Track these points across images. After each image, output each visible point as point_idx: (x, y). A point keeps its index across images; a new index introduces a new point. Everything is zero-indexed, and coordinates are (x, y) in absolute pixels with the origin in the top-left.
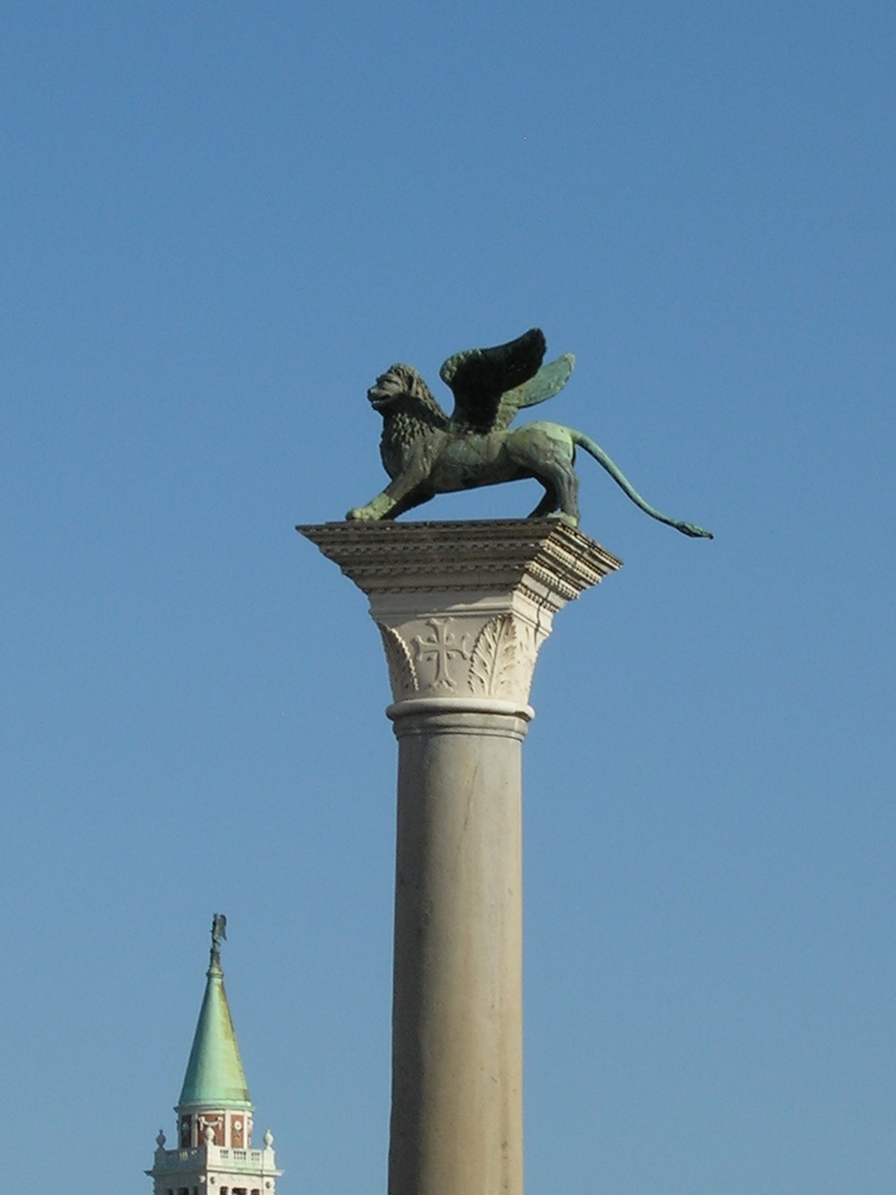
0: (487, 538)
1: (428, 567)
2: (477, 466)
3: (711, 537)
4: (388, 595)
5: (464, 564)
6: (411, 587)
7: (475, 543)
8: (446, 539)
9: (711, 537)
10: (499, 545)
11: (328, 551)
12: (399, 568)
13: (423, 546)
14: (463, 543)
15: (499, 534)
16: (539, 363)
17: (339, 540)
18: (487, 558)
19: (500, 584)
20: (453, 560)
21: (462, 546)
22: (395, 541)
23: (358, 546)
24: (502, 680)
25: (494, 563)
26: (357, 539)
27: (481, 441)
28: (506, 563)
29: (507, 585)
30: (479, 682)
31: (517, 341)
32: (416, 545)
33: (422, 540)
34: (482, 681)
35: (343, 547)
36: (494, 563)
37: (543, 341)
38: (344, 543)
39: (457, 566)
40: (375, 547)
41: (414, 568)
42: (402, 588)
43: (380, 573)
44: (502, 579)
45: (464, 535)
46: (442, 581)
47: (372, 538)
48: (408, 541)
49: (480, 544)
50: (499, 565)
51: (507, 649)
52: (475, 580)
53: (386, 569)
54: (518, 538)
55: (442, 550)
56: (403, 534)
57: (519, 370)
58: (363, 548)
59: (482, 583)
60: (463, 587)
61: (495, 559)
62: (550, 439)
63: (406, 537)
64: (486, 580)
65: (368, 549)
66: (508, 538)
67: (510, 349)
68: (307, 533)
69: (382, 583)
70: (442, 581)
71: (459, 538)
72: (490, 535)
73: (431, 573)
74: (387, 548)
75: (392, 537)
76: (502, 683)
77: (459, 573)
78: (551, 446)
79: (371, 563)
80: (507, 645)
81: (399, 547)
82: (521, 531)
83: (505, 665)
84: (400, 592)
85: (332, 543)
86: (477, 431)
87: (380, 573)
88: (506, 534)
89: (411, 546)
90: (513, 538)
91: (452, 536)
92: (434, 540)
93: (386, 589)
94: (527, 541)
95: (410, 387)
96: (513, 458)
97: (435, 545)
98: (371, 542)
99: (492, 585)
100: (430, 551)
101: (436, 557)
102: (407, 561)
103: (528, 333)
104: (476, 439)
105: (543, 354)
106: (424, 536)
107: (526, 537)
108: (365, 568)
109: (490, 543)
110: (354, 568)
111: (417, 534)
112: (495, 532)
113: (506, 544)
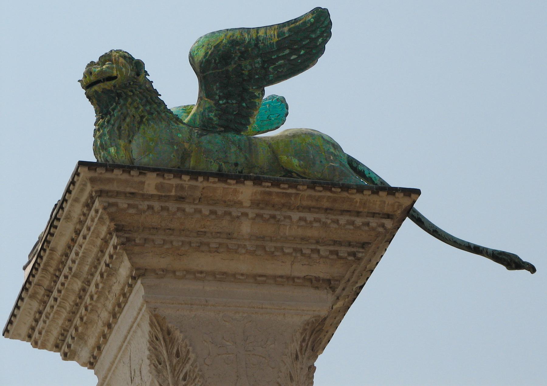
0: (319, 209)
2: (236, 165)
3: (532, 269)
6: (201, 272)
7: (302, 215)
9: (532, 269)
11: (110, 205)
13: (235, 212)
16: (321, 50)
17: (128, 190)
19: (318, 279)
21: (285, 217)
25: (319, 247)
27: (238, 137)
28: (332, 248)
29: (324, 280)
31: (296, 20)
32: (226, 209)
35: (131, 202)
36: (319, 247)
40: (173, 206)
42: (188, 272)
44: (321, 270)
46: (243, 265)
49: (310, 217)
50: (324, 250)
54: (358, 214)
57: (293, 57)
58: (157, 205)
59: (296, 274)
61: (317, 242)
62: (328, 142)
66: (343, 212)
67: (286, 29)
68: (92, 174)
70: (243, 265)
72: (326, 204)
74: (189, 209)
75: (198, 194)
78: (332, 150)
84: (183, 277)
88: (346, 207)
89: (220, 210)
94: (370, 219)
95: (138, 74)
96: (284, 158)
103: (312, 12)
104: (231, 135)
105: (325, 41)
106: (240, 197)
108: (151, 237)
109: (322, 217)
112: (335, 200)
113: (343, 219)
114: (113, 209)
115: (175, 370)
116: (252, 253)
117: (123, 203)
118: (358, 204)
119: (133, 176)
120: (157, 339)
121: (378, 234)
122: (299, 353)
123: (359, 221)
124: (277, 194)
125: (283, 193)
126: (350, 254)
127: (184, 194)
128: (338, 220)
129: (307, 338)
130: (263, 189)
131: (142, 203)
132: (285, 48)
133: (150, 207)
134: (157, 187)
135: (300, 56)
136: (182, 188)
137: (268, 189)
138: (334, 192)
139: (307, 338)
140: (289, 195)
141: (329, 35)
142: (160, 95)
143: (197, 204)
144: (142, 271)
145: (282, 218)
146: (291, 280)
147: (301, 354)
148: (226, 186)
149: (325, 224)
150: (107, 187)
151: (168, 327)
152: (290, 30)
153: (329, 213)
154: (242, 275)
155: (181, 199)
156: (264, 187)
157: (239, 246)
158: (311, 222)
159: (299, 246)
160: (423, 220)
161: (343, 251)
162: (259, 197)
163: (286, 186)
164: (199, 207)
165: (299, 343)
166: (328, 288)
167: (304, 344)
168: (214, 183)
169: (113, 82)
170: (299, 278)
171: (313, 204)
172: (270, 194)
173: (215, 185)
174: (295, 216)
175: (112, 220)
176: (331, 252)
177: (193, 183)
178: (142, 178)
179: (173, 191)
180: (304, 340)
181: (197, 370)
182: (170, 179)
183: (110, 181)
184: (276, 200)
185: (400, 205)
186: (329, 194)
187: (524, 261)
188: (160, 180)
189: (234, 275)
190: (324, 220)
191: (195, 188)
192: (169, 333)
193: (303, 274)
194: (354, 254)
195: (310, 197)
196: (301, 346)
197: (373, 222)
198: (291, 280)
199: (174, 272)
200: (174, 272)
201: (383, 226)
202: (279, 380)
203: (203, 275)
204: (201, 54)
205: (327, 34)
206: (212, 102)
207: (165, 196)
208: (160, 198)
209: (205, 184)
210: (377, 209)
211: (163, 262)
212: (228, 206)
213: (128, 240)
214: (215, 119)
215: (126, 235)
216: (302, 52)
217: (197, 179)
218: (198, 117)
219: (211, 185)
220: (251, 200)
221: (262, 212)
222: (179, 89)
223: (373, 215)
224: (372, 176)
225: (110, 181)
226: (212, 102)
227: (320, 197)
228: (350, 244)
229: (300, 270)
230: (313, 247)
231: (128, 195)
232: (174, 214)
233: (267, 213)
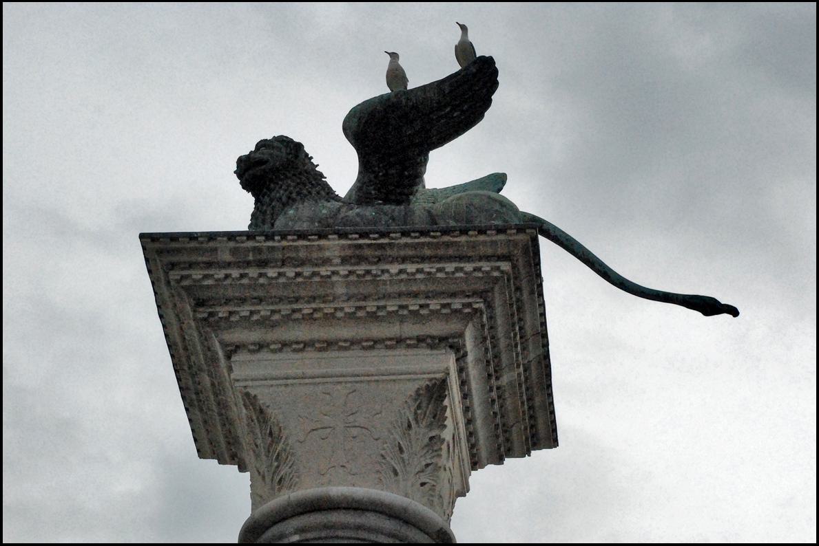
0: (423, 259)
1: (328, 308)
4: (264, 355)
5: (382, 303)
6: (297, 343)
7: (402, 267)
8: (361, 259)
10: (439, 270)
12: (285, 308)
13: (324, 271)
14: (387, 267)
15: (441, 252)
16: (487, 103)
18: (416, 295)
19: (433, 338)
20: (365, 298)
21: (383, 271)
22: (283, 263)
23: (228, 271)
24: (424, 481)
26: (227, 257)
30: (392, 475)
33: (326, 261)
34: (396, 473)
36: (428, 302)
37: (496, 72)
38: (209, 265)
39: (371, 306)
40: (253, 272)
41: (307, 309)
42: (285, 345)
43: (255, 317)
44: (436, 328)
45: (389, 252)
47: (251, 258)
48: (303, 263)
49: (411, 268)
50: (434, 304)
51: (431, 438)
52: (393, 330)
53: (264, 310)
54: (469, 259)
55: (353, 278)
56: (296, 249)
58: (235, 273)
60: (377, 342)
61: (427, 297)
63: (302, 254)
64: (411, 329)
65: (242, 276)
66: (450, 259)
68: (157, 245)
69: (255, 336)
71: (380, 260)
72: (428, 252)
73: (330, 318)
74: (272, 273)
75: (279, 255)
76: (423, 484)
77: (373, 316)
79: (243, 301)
80: (433, 434)
81: (290, 272)
82: (473, 246)
83: (429, 461)
85: (191, 265)
86: (387, 201)
87: (255, 317)
88: (451, 252)
89: (307, 271)
90: (461, 258)
91: (367, 252)
92: (345, 261)
93: (261, 346)
94: (481, 264)
95: (297, 157)
97: (343, 270)
98: (248, 264)
99: (420, 340)
100: (335, 278)
101: (340, 290)
102: (297, 300)
106: (327, 254)
107: (481, 259)
109: (426, 267)
110: (218, 309)
111: (320, 248)
112: (437, 246)
113: (450, 267)
114: (186, 283)
115: (269, 452)
116: (351, 316)
117: (197, 274)
118: (466, 248)
119: (202, 243)
120: (252, 421)
121: (497, 279)
122: (413, 423)
123: (469, 267)
124: (369, 246)
125: (375, 244)
126: (464, 305)
127: (264, 257)
128: (444, 268)
129: (424, 405)
130: (349, 242)
131: (218, 272)
132: (445, 106)
133: (227, 276)
134: (234, 251)
135: (463, 112)
136: (258, 250)
137: (356, 242)
138: (434, 237)
139: (424, 405)
140: (381, 246)
141: (494, 85)
142: (326, 178)
143: (281, 267)
144: (233, 348)
145: (379, 273)
146: (399, 341)
147: (417, 422)
148: (308, 243)
149: (429, 273)
150: (175, 259)
151: (260, 407)
152: (451, 85)
153: (434, 262)
154: (345, 341)
155: (263, 264)
156: (351, 239)
157: (336, 309)
158: (413, 274)
159: (405, 303)
160: (609, 273)
161: (457, 303)
162: (349, 252)
163: (376, 236)
164: (282, 270)
165: (412, 410)
166: (447, 348)
167: (419, 412)
168: (293, 240)
169: (263, 167)
170: (410, 339)
171: (410, 253)
172: (360, 247)
173: (295, 244)
174: (394, 269)
175: (189, 295)
176: (444, 306)
177: (270, 244)
178: (211, 244)
179: (251, 254)
180: (419, 407)
181: (288, 448)
182: (243, 242)
183: (178, 251)
184: (367, 252)
185: (516, 244)
186: (428, 240)
187: (723, 303)
188: (232, 244)
189: (336, 343)
190: (428, 270)
191: (273, 248)
192: (261, 411)
193: (416, 334)
194: (469, 305)
195: (406, 245)
196: (416, 413)
197: (486, 266)
198: (399, 341)
199: (268, 345)
200: (268, 345)
201: (498, 268)
202: (383, 452)
203: (301, 346)
204: (354, 124)
205: (493, 85)
206: (372, 176)
207: (244, 262)
208: (238, 265)
209: (284, 243)
210: (490, 251)
211: (255, 336)
212: (317, 265)
213: (211, 314)
214: (373, 192)
215: (210, 310)
216: (466, 107)
217: (273, 239)
218: (354, 192)
219: (291, 243)
220: (340, 256)
221: (355, 268)
222: (340, 168)
223: (488, 258)
224: (557, 233)
225: (178, 251)
226: (372, 176)
227: (418, 244)
228: (463, 294)
229: (411, 329)
230: (422, 302)
231: (202, 265)
232: (257, 279)
233: (360, 269)
